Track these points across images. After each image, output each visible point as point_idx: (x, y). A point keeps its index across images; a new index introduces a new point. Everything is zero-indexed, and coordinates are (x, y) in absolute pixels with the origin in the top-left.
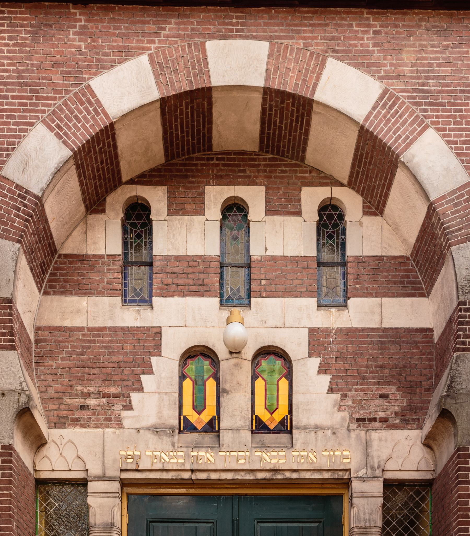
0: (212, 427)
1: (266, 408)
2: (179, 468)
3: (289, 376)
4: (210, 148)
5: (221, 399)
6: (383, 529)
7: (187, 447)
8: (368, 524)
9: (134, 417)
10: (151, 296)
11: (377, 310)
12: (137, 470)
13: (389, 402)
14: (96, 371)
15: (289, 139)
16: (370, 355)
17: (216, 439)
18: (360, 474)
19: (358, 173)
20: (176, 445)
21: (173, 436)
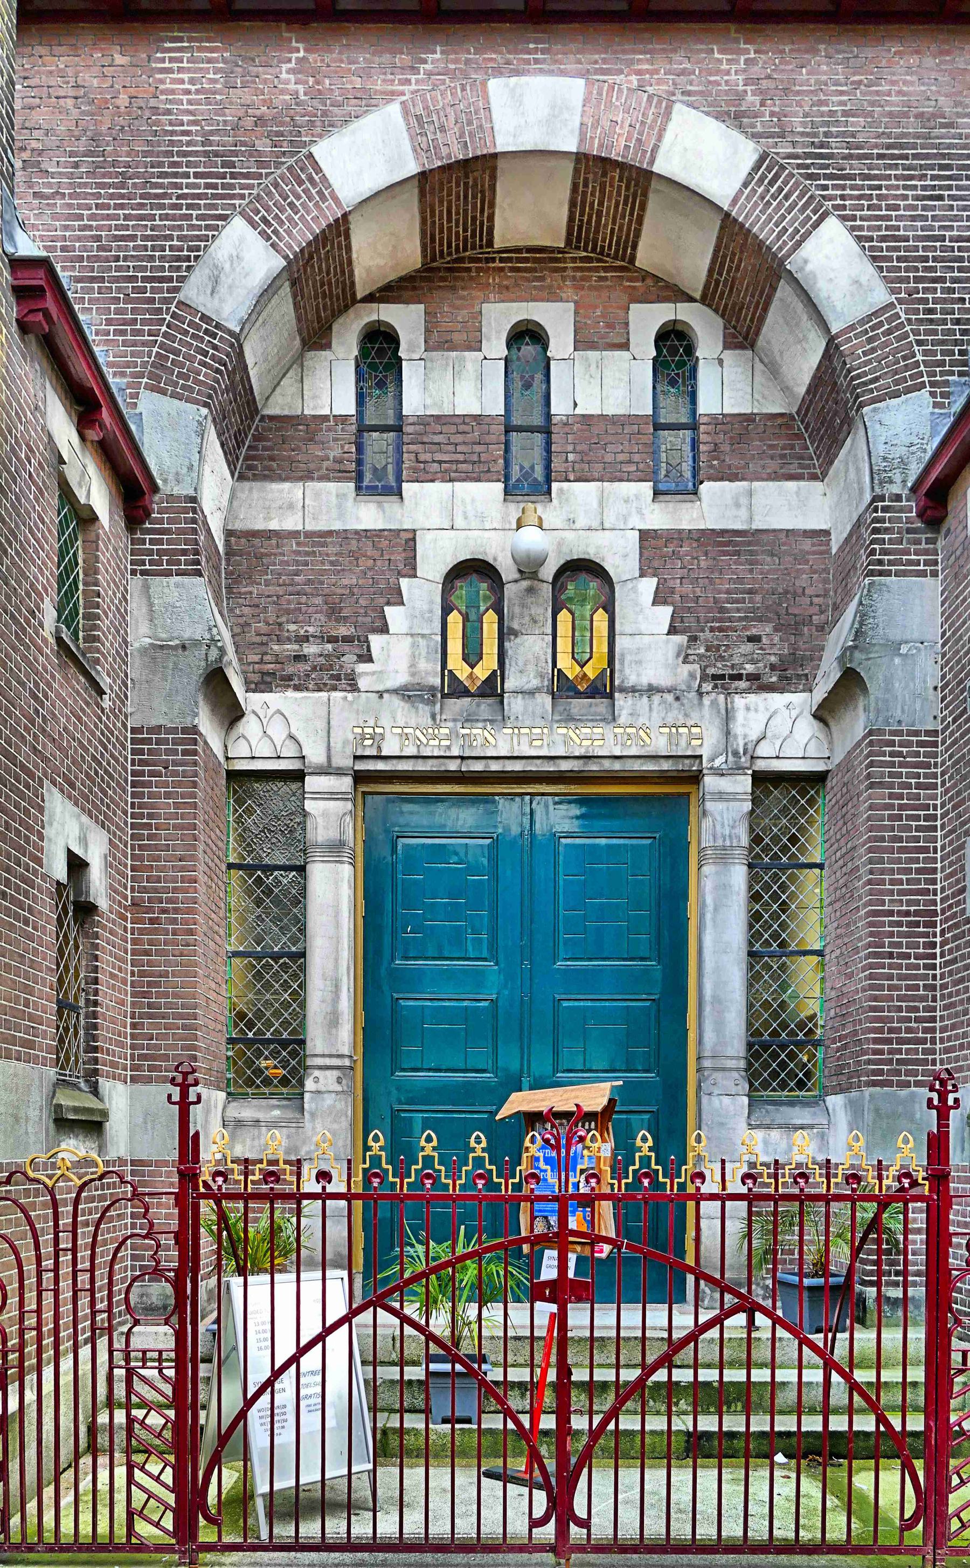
0: (492, 689)
1: (573, 657)
2: (442, 754)
3: (609, 607)
4: (490, 243)
5: (507, 644)
6: (751, 849)
7: (455, 720)
8: (728, 843)
9: (373, 673)
10: (400, 481)
11: (744, 501)
12: (380, 758)
13: (761, 649)
14: (318, 600)
15: (613, 230)
16: (733, 573)
17: (497, 707)
18: (717, 763)
19: (717, 282)
20: (438, 717)
21: (434, 703)
